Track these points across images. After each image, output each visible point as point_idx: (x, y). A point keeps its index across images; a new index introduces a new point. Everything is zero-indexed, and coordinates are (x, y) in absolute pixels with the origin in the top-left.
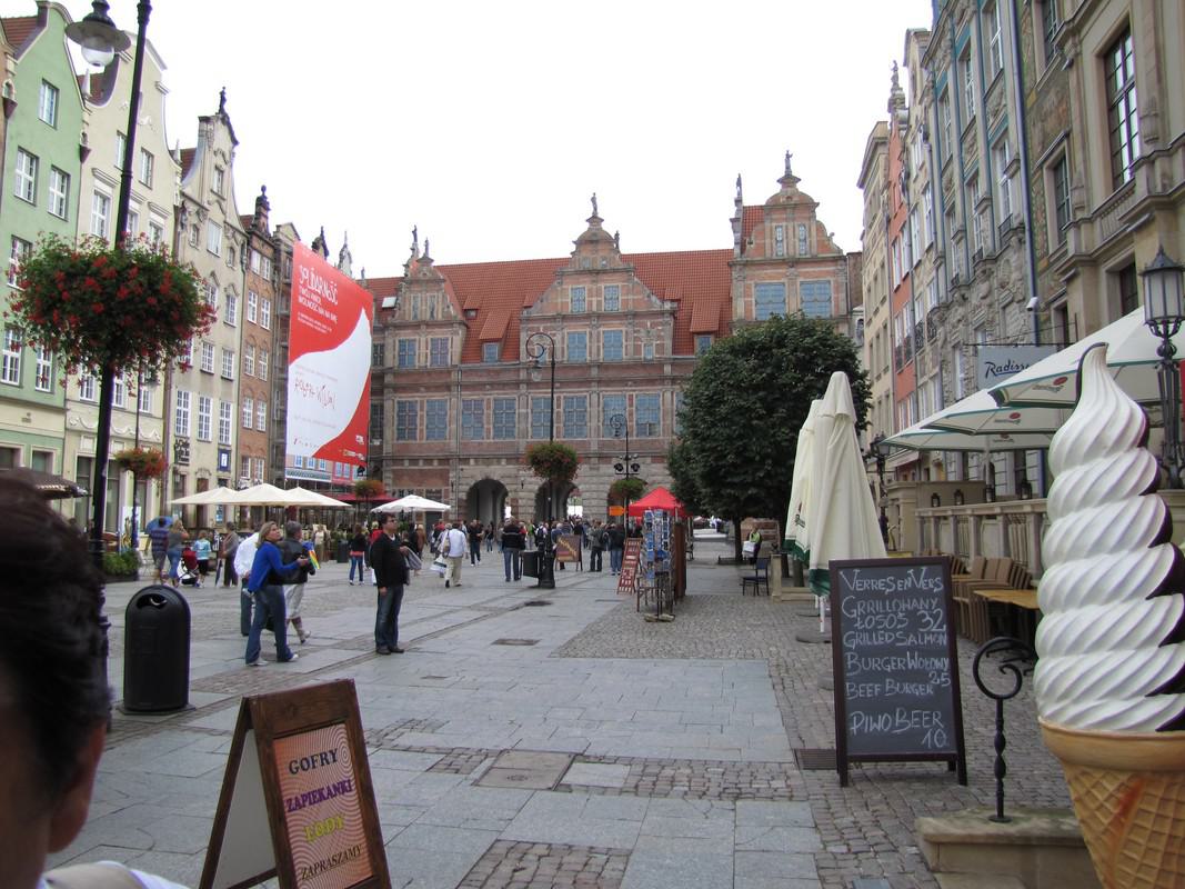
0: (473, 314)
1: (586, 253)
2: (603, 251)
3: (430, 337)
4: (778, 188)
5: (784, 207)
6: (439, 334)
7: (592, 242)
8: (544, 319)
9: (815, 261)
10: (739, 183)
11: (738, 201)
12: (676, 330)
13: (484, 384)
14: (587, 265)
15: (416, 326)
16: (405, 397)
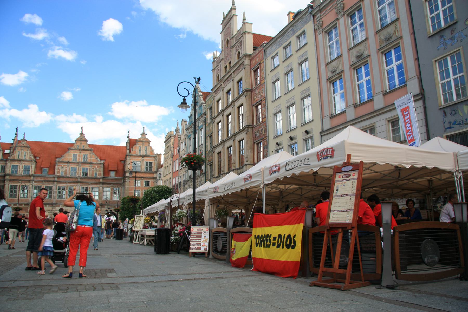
0: (38, 158)
1: (79, 143)
2: (84, 143)
3: (24, 165)
4: (140, 136)
5: (142, 141)
6: (27, 164)
7: (80, 141)
8: (63, 162)
9: (149, 156)
10: (129, 132)
11: (128, 137)
12: (104, 169)
13: (42, 181)
14: (79, 148)
15: (19, 161)
16: (14, 184)
